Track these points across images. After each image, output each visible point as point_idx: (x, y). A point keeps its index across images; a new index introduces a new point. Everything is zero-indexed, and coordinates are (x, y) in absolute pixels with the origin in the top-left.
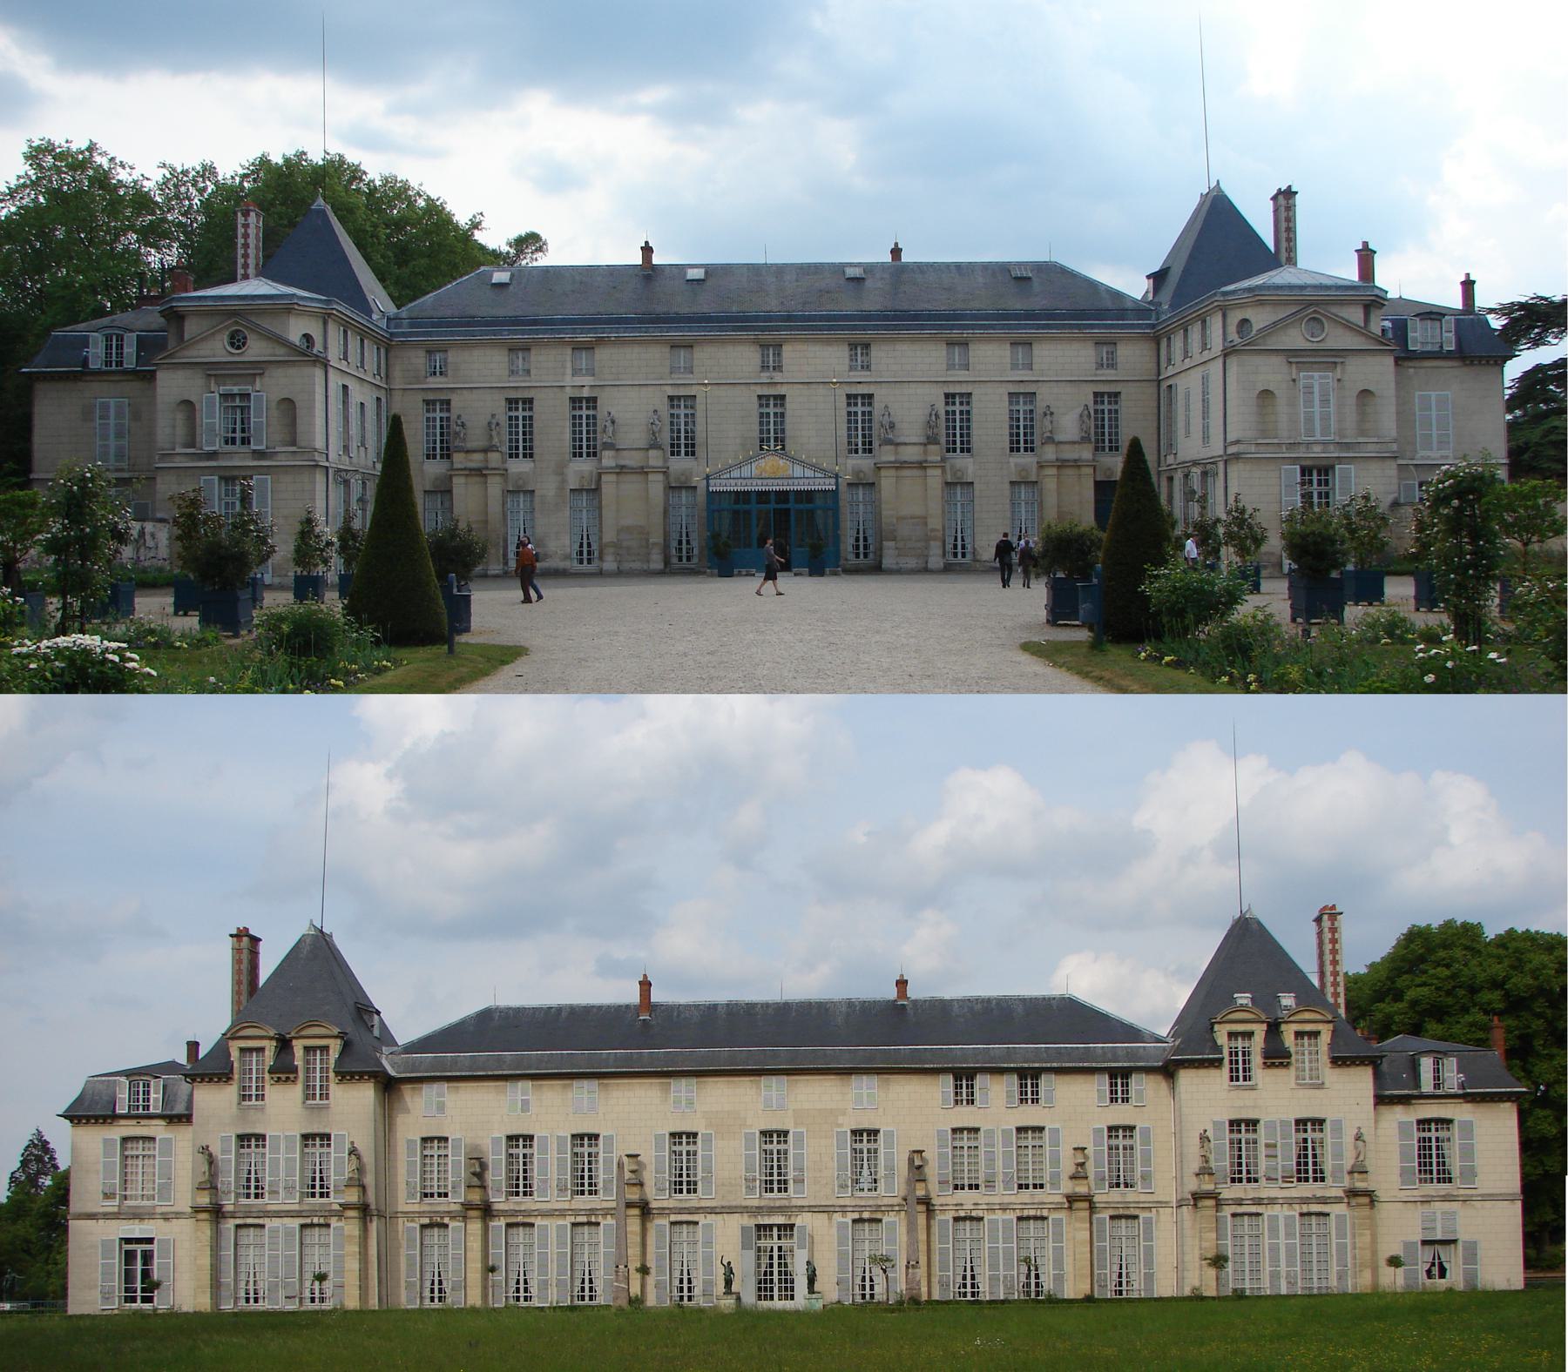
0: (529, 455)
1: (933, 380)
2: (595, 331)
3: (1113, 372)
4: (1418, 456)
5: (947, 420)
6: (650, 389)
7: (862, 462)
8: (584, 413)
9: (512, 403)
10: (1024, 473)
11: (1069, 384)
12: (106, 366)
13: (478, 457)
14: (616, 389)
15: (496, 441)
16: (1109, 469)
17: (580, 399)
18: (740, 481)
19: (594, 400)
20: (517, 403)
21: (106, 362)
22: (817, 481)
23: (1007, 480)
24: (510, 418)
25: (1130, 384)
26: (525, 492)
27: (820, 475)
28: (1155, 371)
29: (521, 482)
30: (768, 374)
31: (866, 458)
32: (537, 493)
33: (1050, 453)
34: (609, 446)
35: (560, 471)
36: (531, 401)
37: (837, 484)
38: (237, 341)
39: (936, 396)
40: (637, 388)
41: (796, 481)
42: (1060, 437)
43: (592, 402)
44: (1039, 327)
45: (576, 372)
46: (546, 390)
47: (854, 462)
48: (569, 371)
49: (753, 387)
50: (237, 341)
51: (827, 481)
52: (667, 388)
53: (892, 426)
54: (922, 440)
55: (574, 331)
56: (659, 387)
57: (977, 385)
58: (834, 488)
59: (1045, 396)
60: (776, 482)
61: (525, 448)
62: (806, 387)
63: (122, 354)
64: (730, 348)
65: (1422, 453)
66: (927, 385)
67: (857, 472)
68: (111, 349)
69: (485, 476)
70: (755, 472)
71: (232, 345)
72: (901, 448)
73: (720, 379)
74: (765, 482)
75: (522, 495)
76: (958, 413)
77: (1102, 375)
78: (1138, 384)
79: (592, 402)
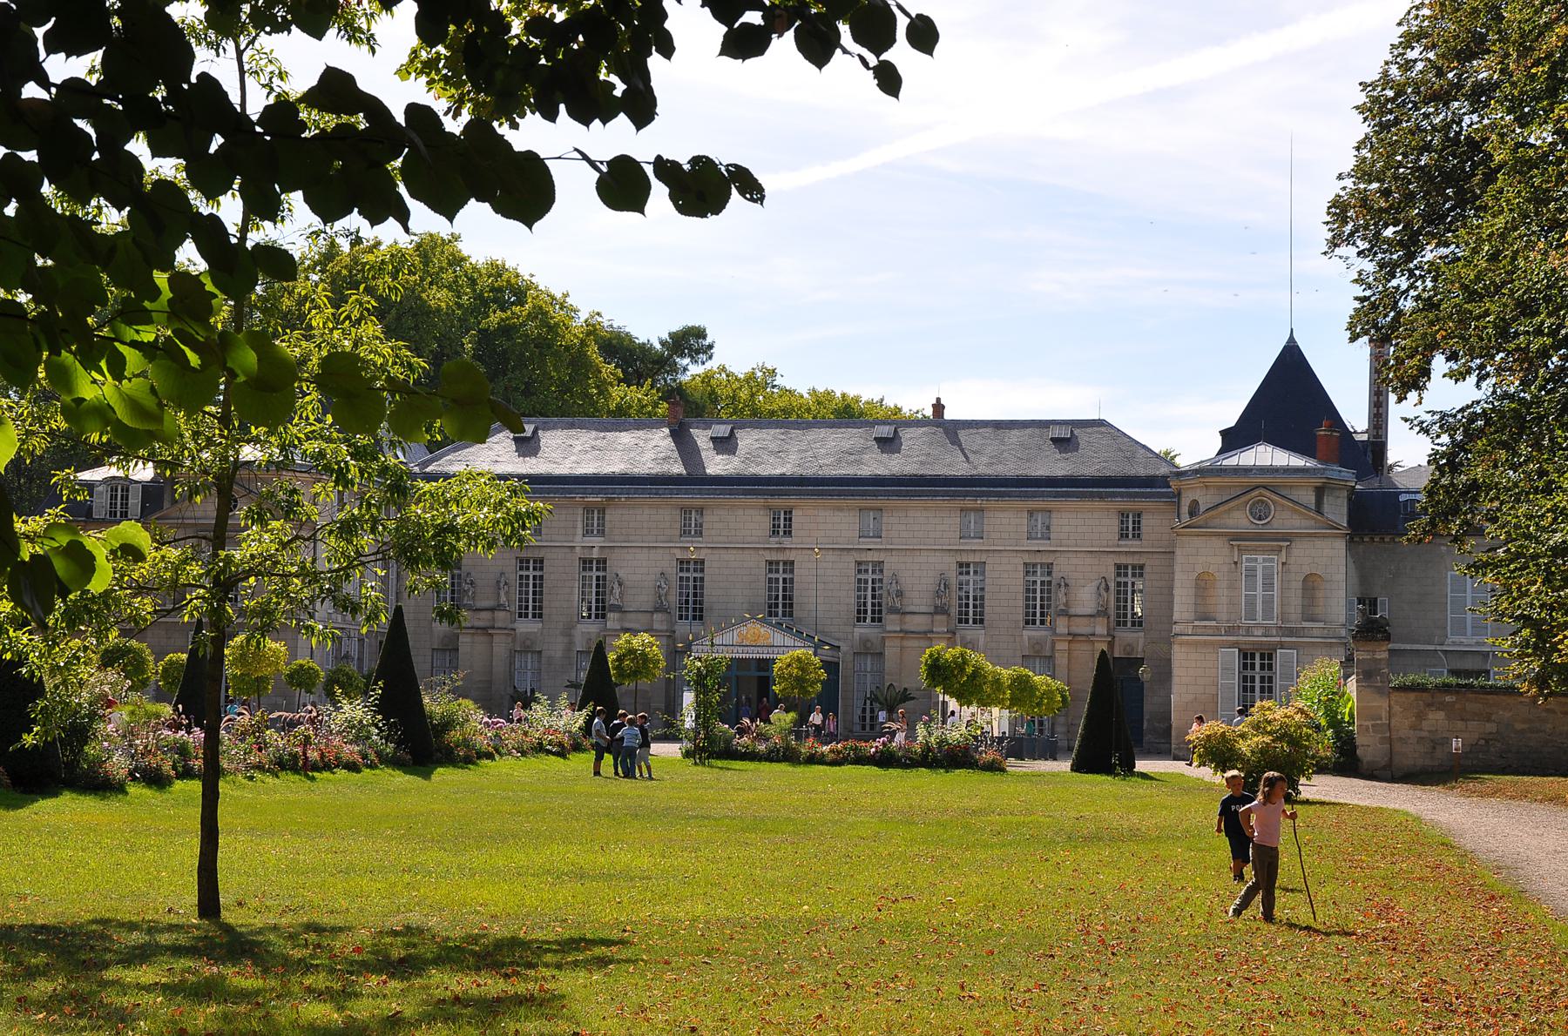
0: (538, 615)
1: (944, 548)
2: (605, 492)
3: (1138, 543)
4: (1449, 641)
5: (1119, 592)
6: (659, 551)
7: (865, 630)
8: (595, 574)
10: (1037, 647)
11: (1089, 555)
12: (110, 516)
13: (485, 615)
15: (503, 599)
16: (1129, 645)
19: (605, 561)
20: (528, 562)
21: (111, 512)
23: (1019, 654)
25: (1155, 556)
26: (533, 652)
29: (528, 643)
30: (777, 539)
31: (875, 627)
32: (544, 654)
33: (1062, 626)
34: (617, 609)
35: (568, 632)
39: (949, 564)
40: (645, 550)
42: (1072, 611)
44: (1057, 495)
45: (588, 532)
46: (557, 550)
47: (862, 631)
48: (580, 531)
52: (676, 551)
53: (900, 594)
54: (932, 610)
55: (585, 492)
59: (1062, 567)
61: (534, 608)
63: (127, 504)
64: (740, 512)
65: (1452, 638)
67: (865, 641)
68: (116, 499)
69: (491, 635)
72: (908, 617)
73: (730, 543)
75: (529, 655)
76: (531, 578)
77: (1126, 546)
78: (1162, 556)
79: (602, 563)
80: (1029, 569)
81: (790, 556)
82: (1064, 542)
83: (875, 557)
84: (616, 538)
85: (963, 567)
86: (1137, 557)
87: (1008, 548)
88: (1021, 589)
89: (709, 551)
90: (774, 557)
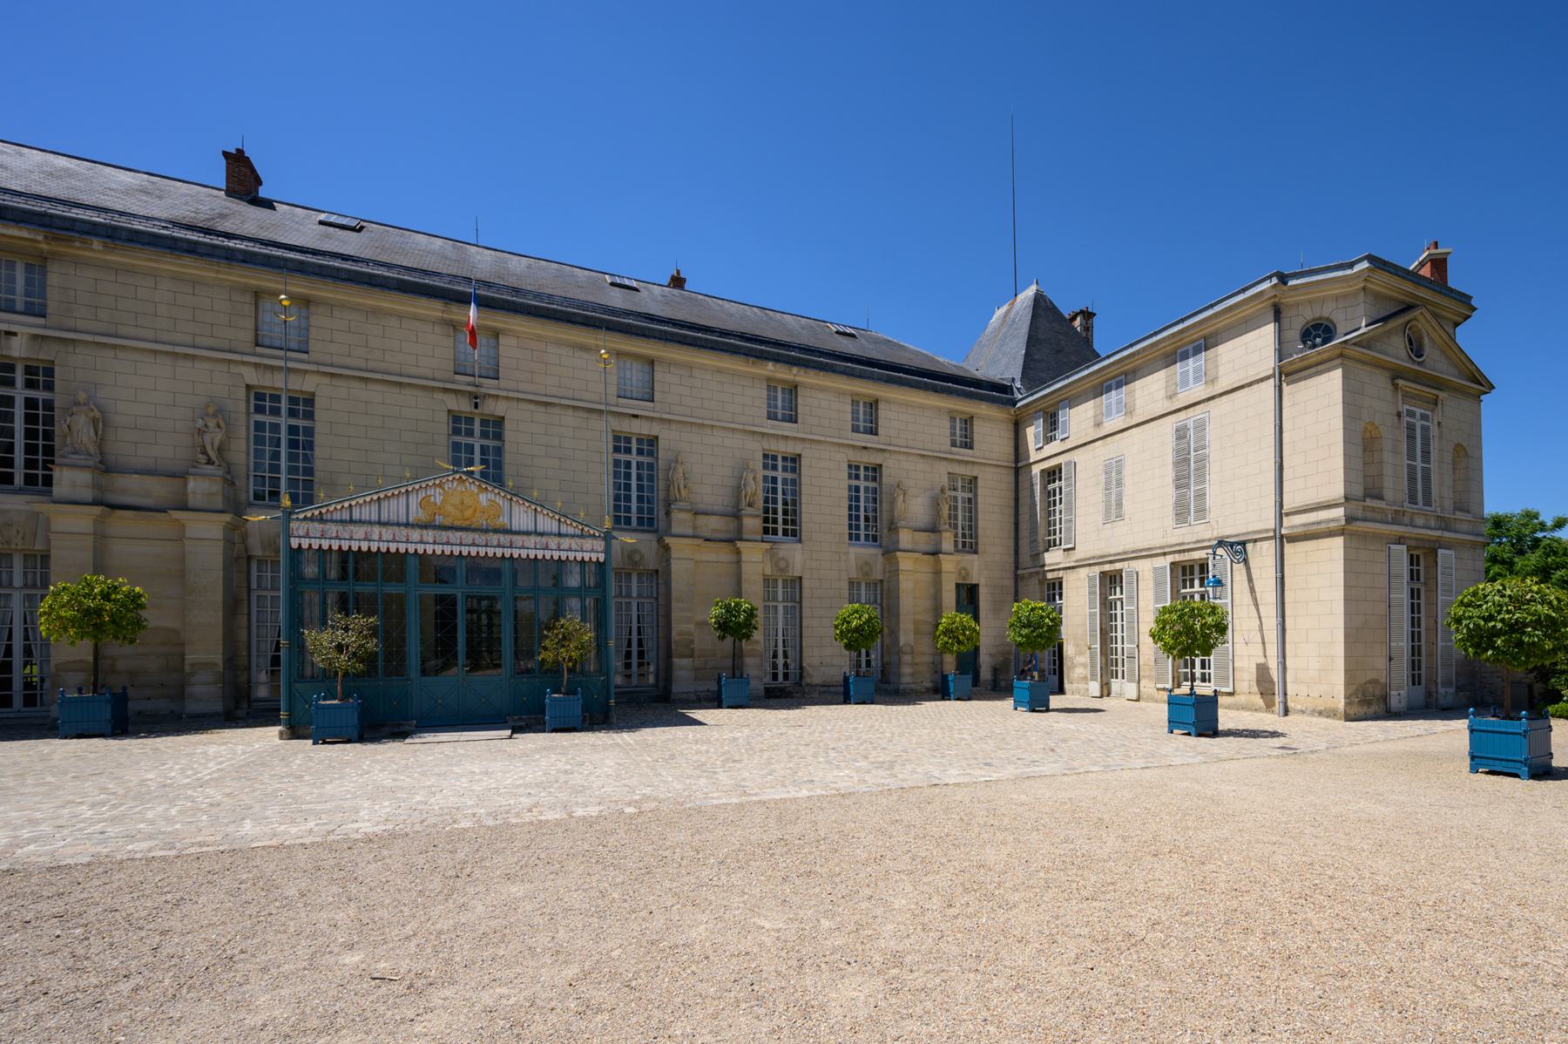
11: (921, 460)
14: (110, 353)
18: (376, 530)
22: (566, 543)
27: (571, 530)
28: (1012, 458)
37: (607, 551)
41: (518, 540)
44: (889, 381)
49: (439, 396)
51: (588, 544)
52: (244, 370)
56: (224, 367)
57: (807, 445)
58: (602, 558)
59: (893, 469)
60: (468, 537)
62: (542, 409)
66: (737, 436)
70: (416, 514)
74: (444, 535)
80: (853, 468)
81: (492, 408)
82: (894, 441)
83: (644, 428)
84: (81, 325)
85: (770, 460)
86: (969, 467)
87: (828, 439)
88: (846, 493)
89: (326, 380)
90: (464, 406)
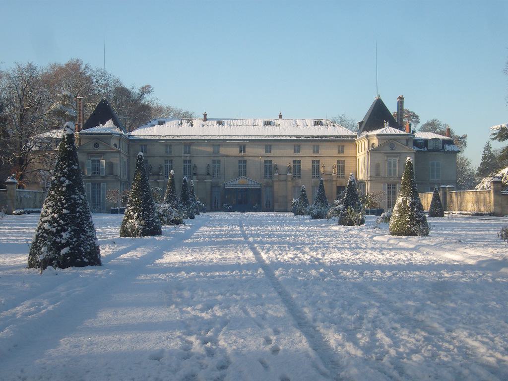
9: (166, 161)
17: (186, 161)
19: (191, 160)
24: (165, 165)
36: (172, 161)
38: (96, 145)
43: (190, 161)
48: (183, 152)
50: (96, 145)
71: (95, 147)
79: (190, 161)
